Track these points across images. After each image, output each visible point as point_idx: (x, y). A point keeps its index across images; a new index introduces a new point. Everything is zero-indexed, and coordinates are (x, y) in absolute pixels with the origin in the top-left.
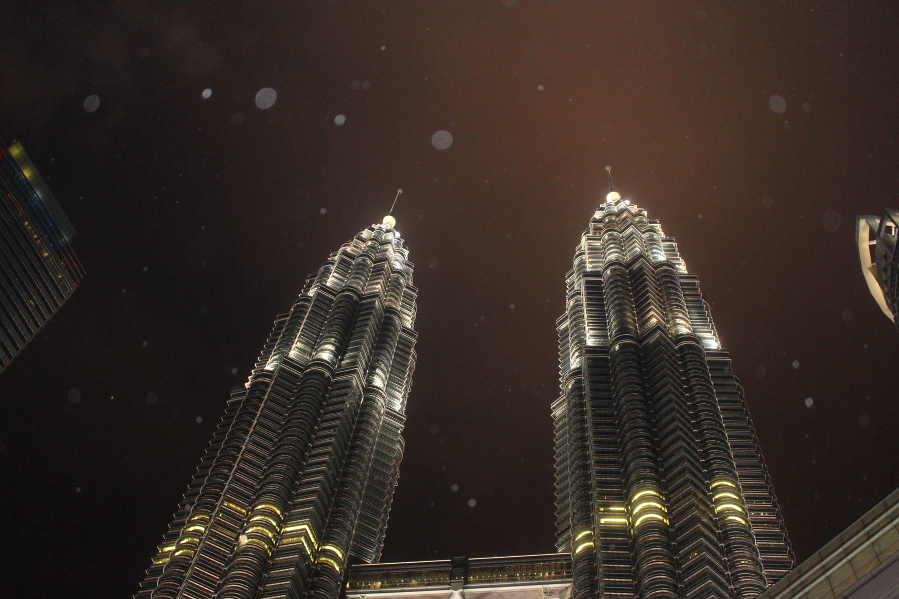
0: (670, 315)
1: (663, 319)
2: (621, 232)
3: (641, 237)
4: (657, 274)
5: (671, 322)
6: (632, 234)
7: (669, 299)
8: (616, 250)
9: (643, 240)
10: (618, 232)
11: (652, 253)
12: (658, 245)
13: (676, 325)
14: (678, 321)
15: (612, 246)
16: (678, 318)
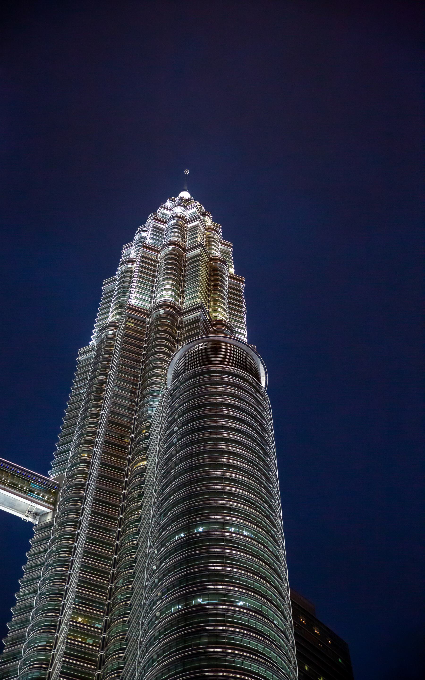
0: (212, 303)
1: (206, 304)
2: (187, 222)
3: (204, 232)
4: (210, 266)
5: (212, 309)
6: (197, 226)
7: (215, 290)
8: (179, 235)
9: (205, 236)
10: (185, 221)
11: (210, 248)
12: (217, 244)
13: (214, 311)
14: (219, 309)
15: (176, 230)
16: (219, 306)
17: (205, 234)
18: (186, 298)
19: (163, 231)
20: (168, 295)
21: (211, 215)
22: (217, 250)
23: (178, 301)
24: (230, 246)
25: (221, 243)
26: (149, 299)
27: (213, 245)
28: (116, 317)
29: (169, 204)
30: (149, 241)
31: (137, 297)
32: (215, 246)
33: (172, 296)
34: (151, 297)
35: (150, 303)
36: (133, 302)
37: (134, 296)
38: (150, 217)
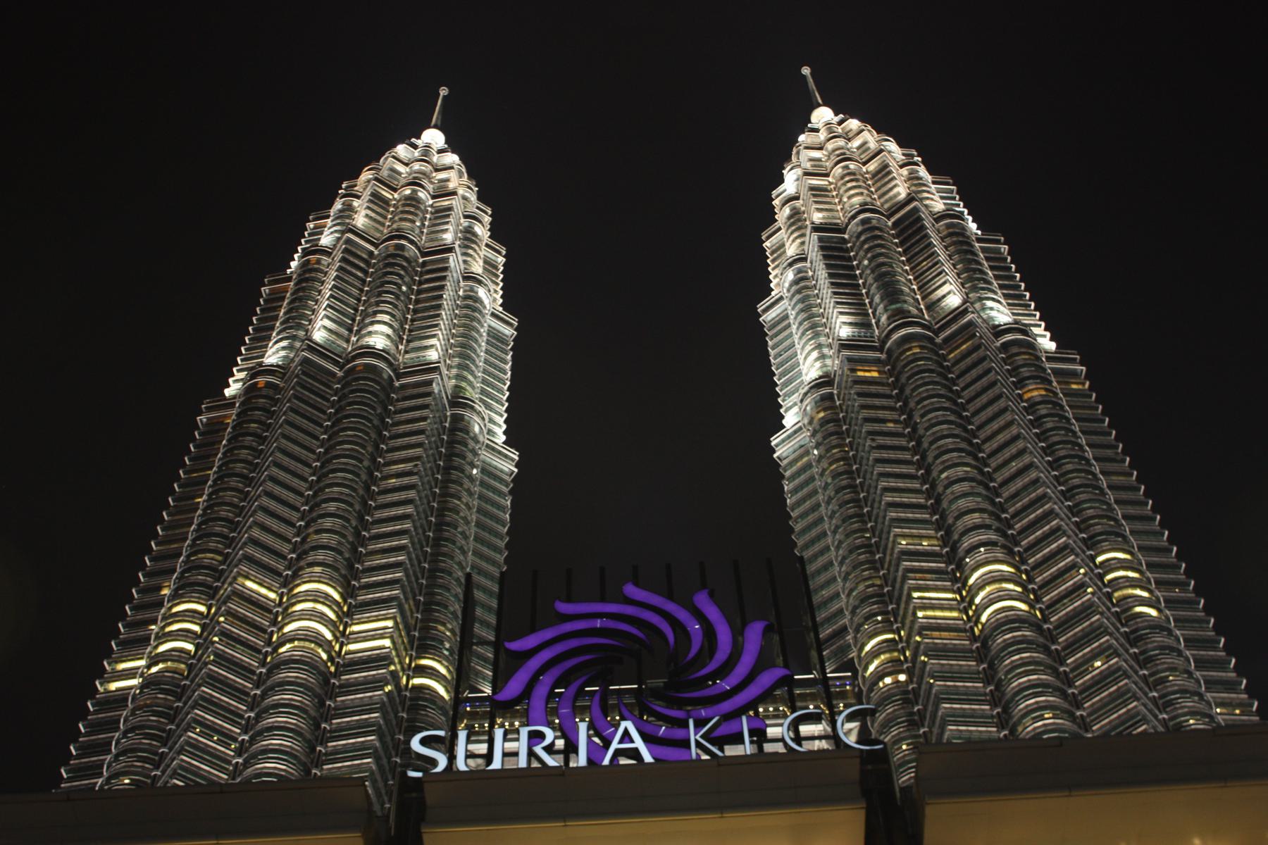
12: (479, 246)
17: (461, 225)
18: (412, 345)
19: (389, 205)
20: (382, 334)
21: (476, 186)
22: (478, 259)
23: (397, 348)
24: (499, 253)
25: (487, 245)
26: (346, 333)
27: (472, 248)
28: (283, 353)
29: (402, 150)
30: (360, 221)
31: (325, 327)
32: (475, 251)
33: (388, 336)
34: (350, 330)
35: (348, 341)
36: (319, 336)
37: (319, 324)
38: (369, 170)
